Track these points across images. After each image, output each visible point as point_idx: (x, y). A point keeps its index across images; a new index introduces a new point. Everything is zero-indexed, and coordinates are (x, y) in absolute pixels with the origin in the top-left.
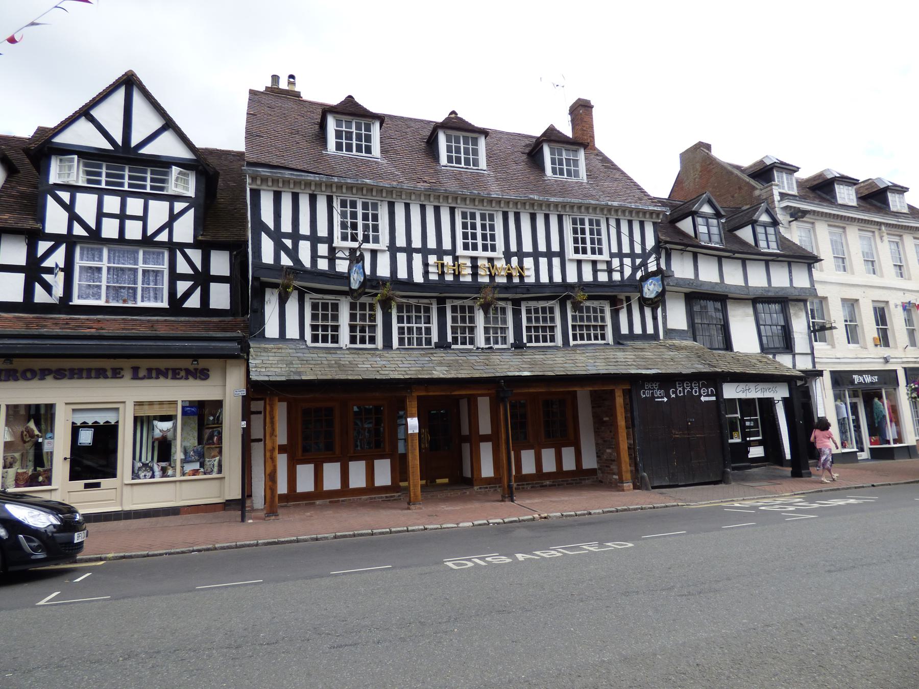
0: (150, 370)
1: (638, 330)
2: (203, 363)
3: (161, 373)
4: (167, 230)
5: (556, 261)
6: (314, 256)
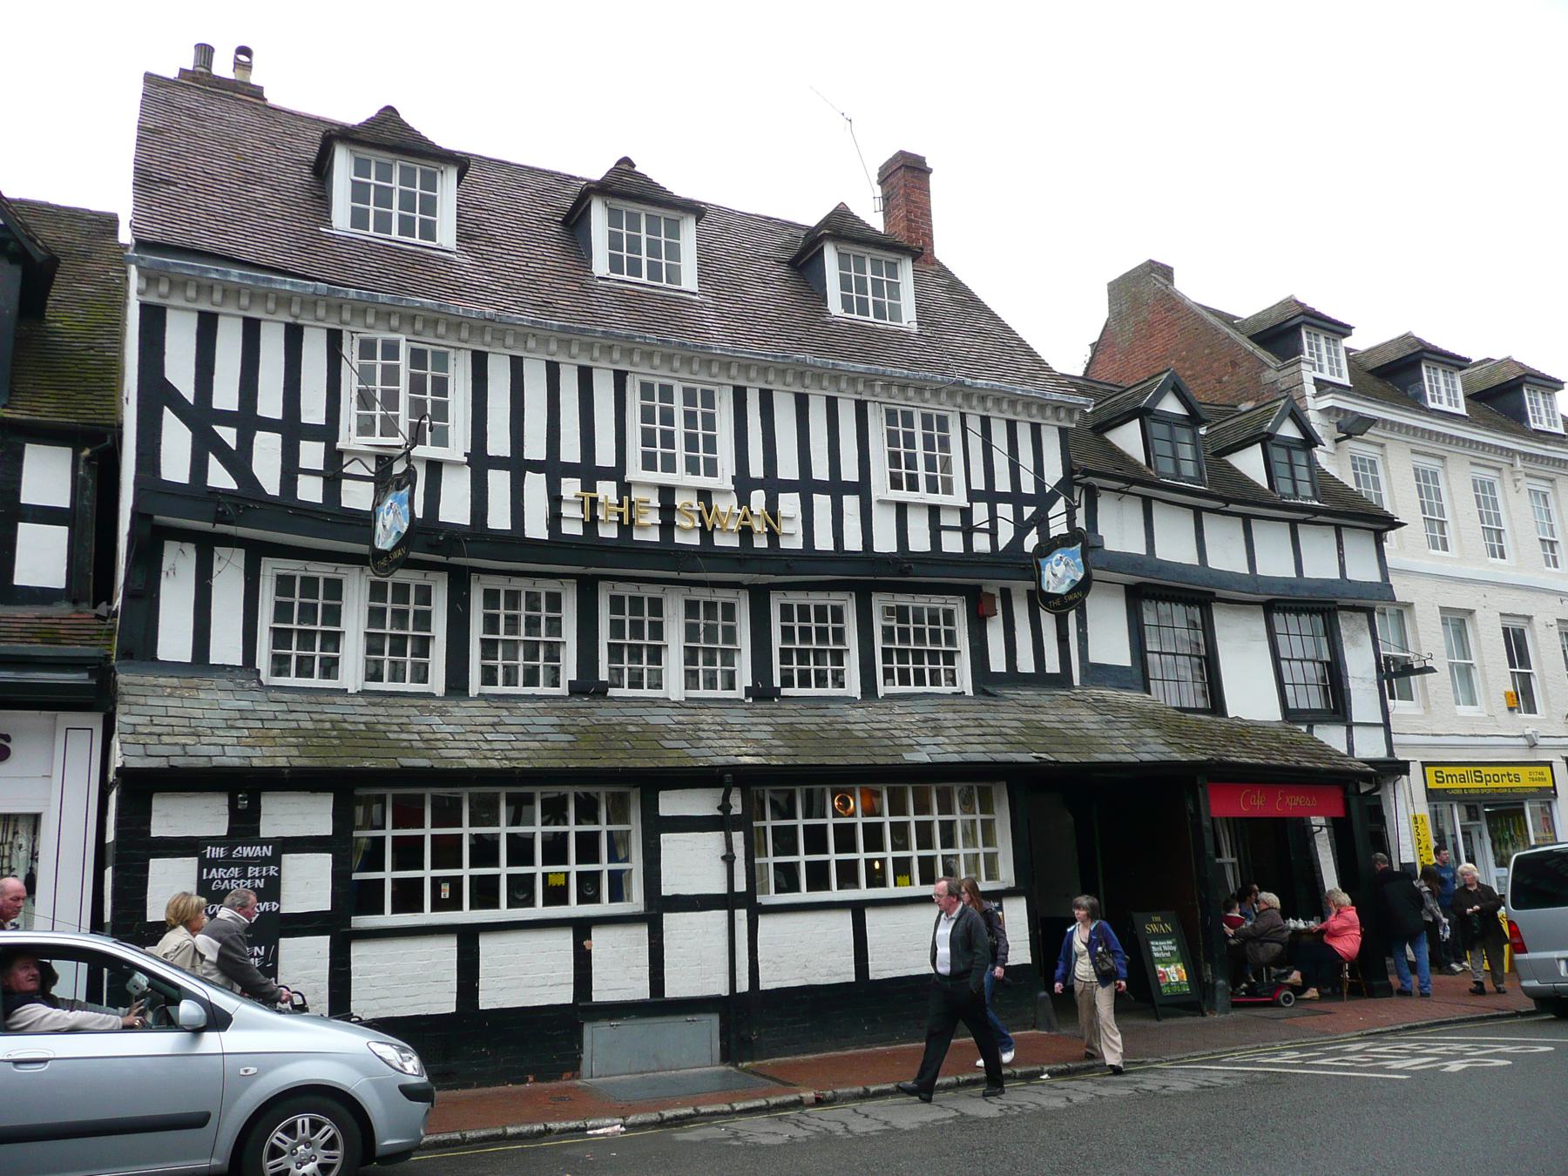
1: (1026, 664)
5: (851, 503)
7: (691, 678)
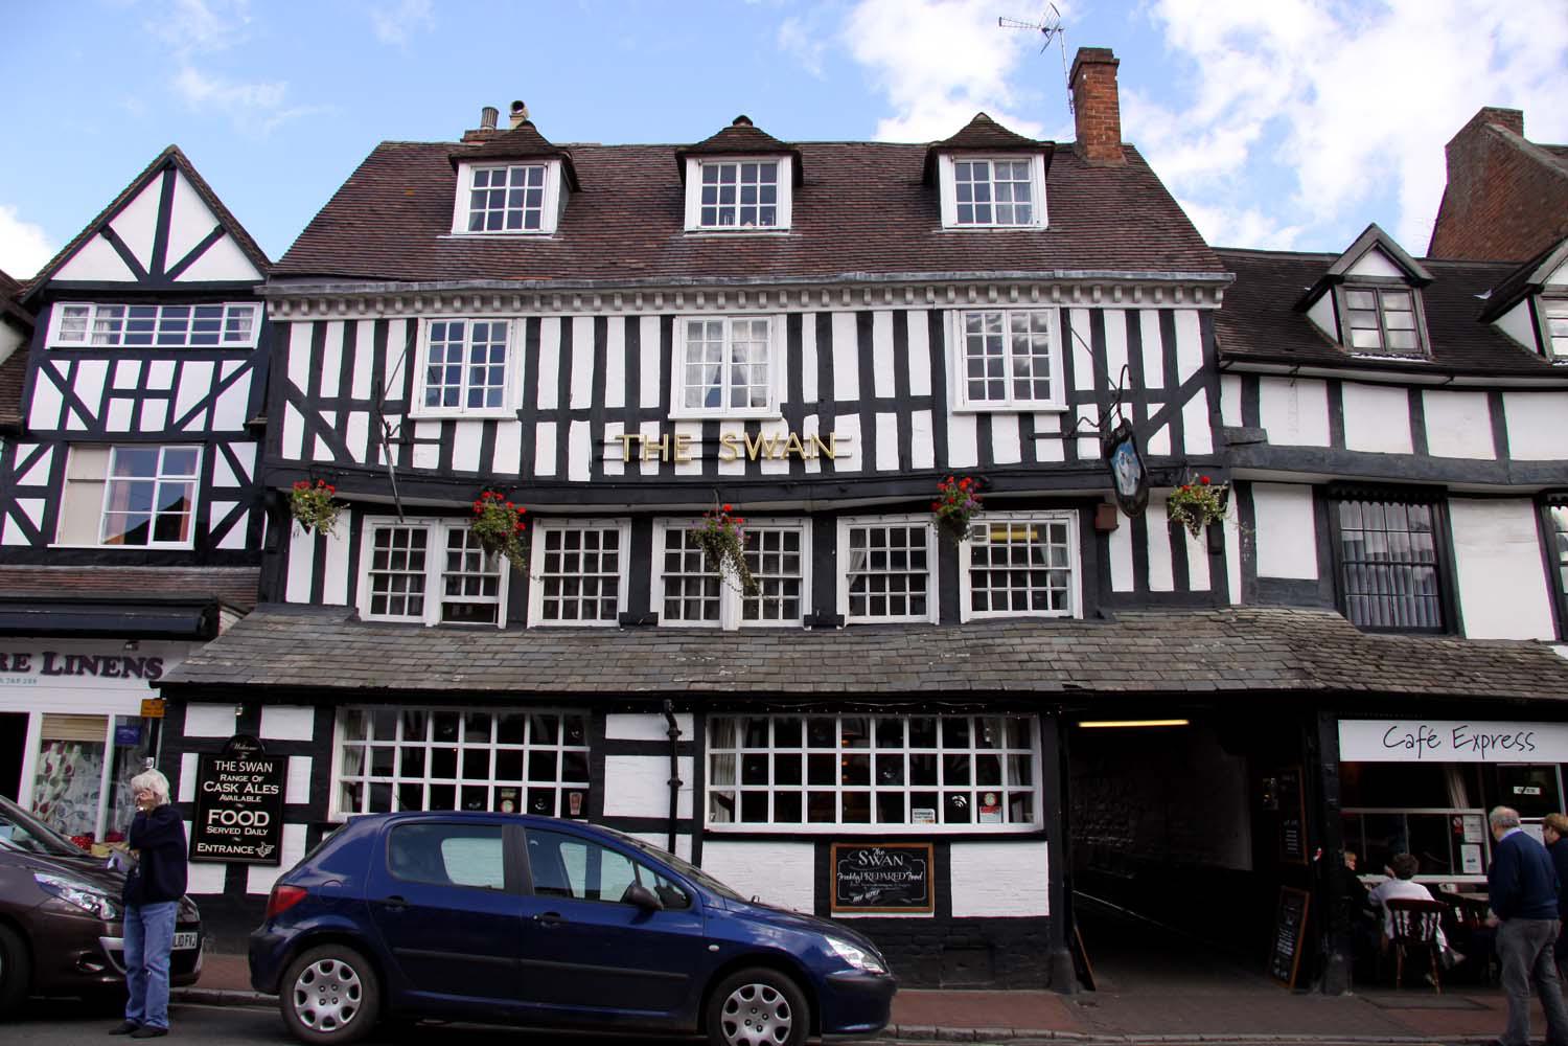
0: (70, 659)
1: (1161, 579)
2: (146, 648)
3: (88, 665)
4: (205, 411)
5: (922, 420)
6: (375, 440)
7: (750, 610)
